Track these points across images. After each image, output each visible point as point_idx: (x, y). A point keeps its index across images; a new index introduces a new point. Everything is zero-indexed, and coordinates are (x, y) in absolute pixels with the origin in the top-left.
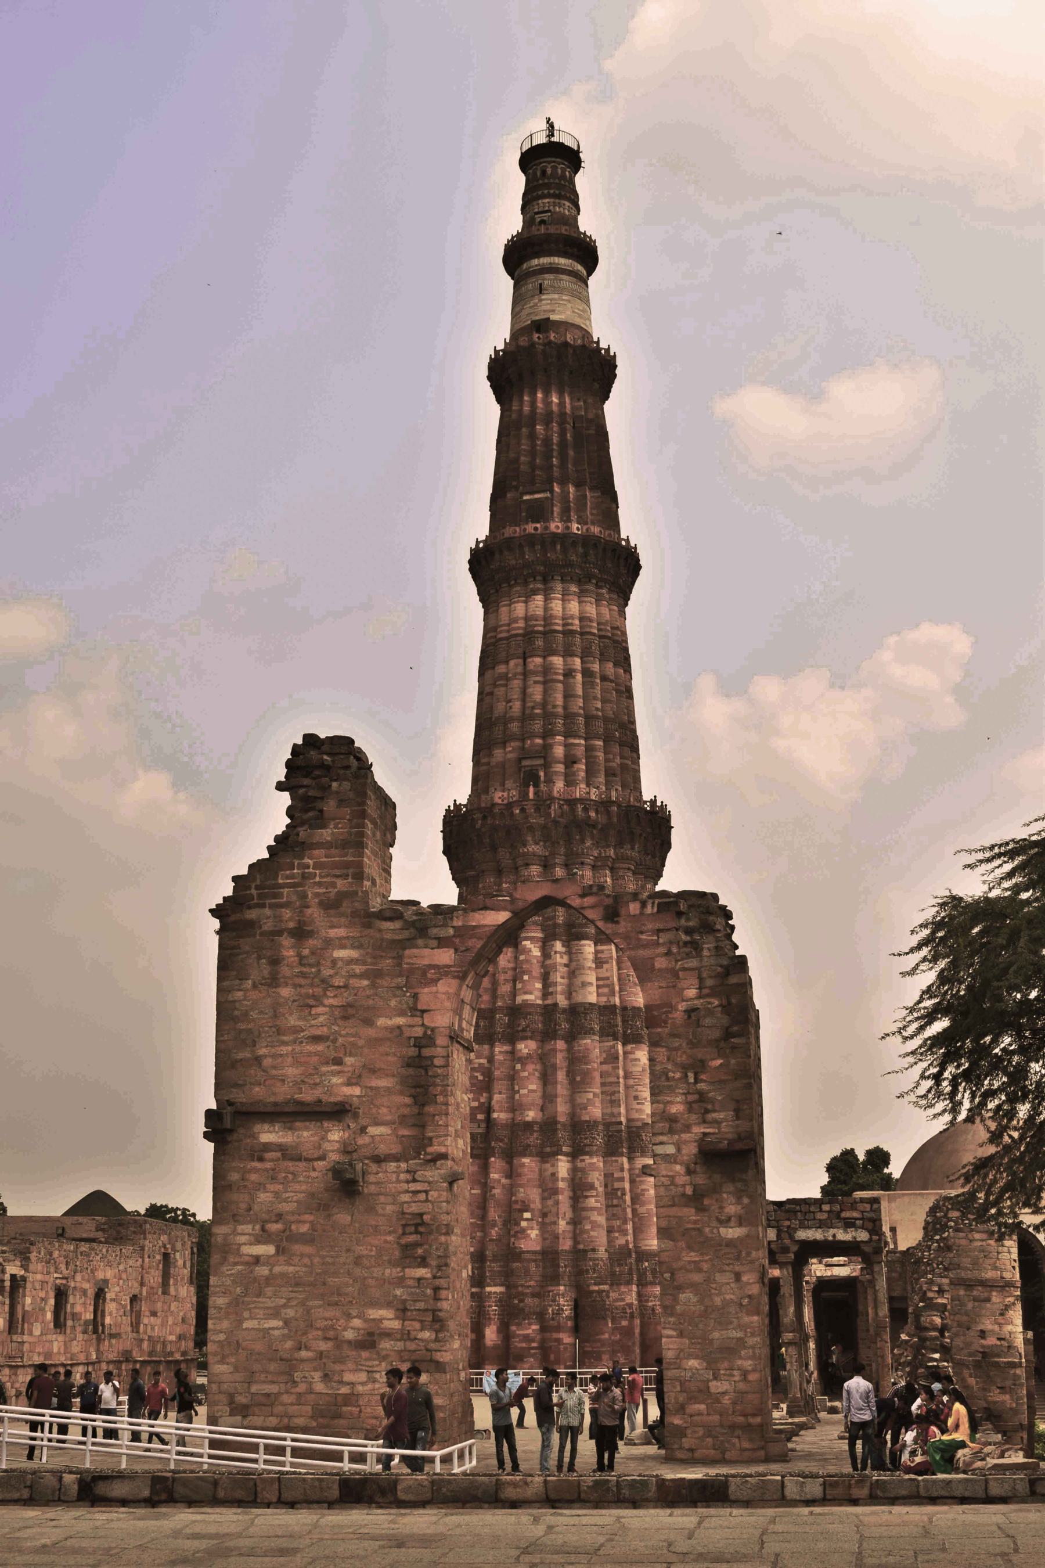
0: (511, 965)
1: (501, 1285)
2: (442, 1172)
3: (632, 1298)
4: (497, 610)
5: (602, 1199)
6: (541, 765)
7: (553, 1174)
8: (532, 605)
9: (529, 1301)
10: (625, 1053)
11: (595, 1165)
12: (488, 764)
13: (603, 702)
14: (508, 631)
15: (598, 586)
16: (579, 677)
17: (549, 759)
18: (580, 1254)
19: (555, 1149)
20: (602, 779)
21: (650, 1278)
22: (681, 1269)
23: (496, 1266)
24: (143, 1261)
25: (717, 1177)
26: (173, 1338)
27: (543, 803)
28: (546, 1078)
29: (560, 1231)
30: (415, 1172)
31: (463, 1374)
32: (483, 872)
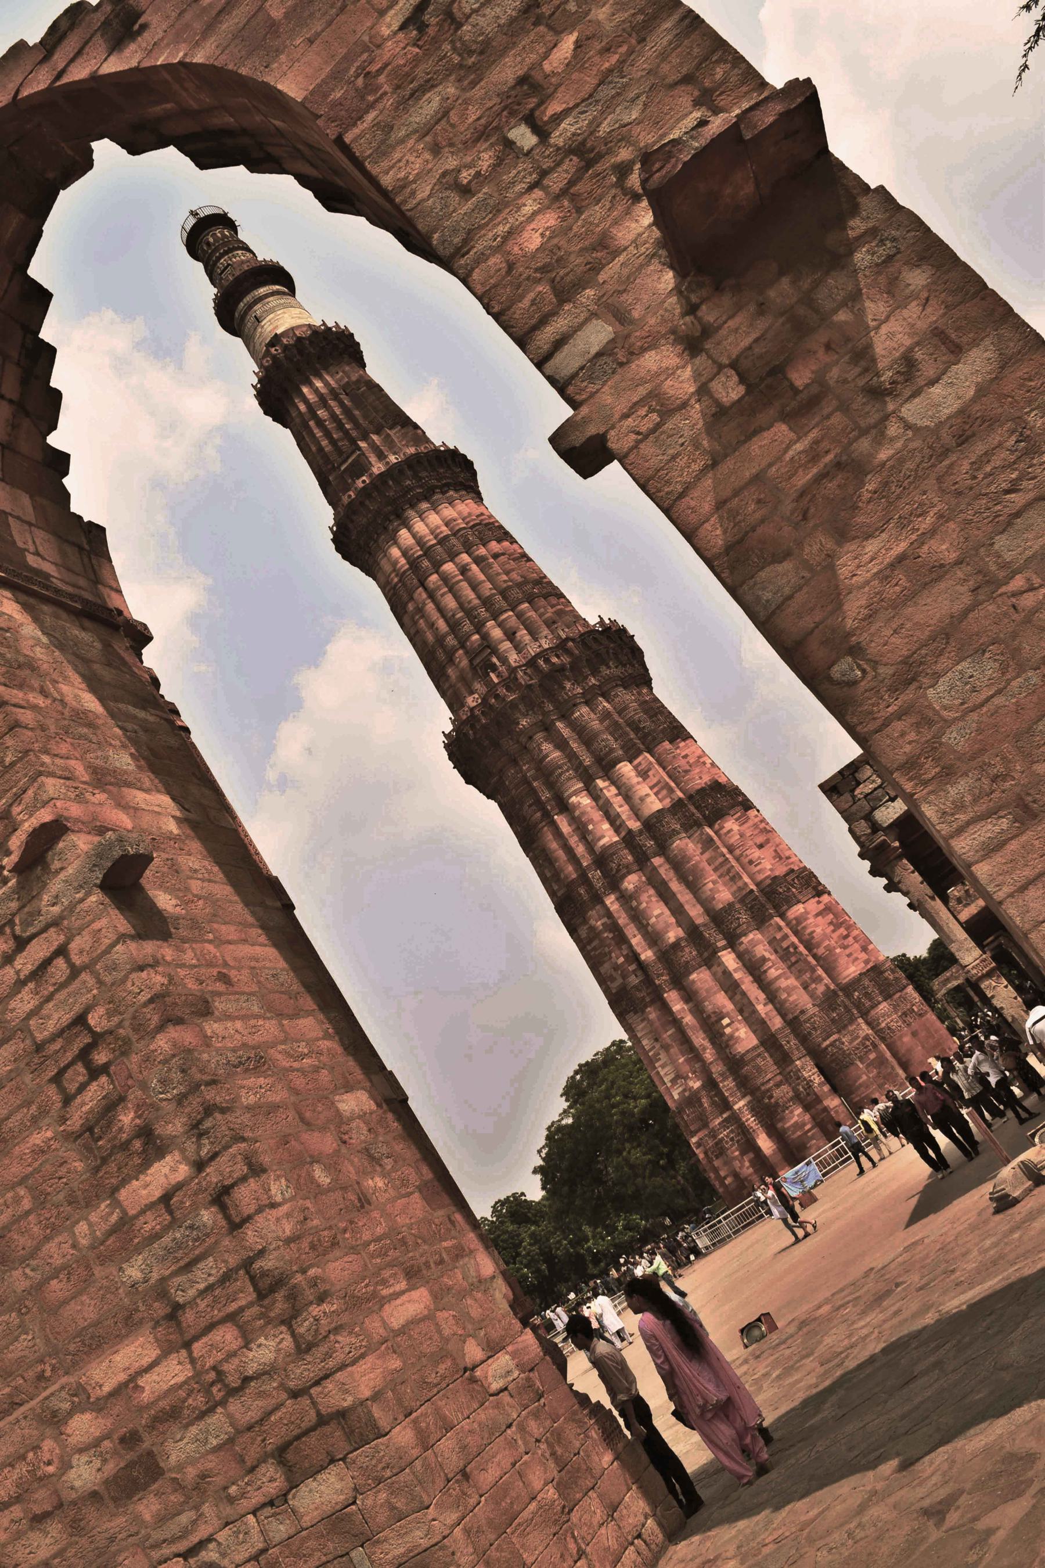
1: (743, 1097)
2: (70, 870)
3: (865, 1030)
8: (401, 541)
9: (777, 1093)
10: (716, 833)
11: (757, 942)
12: (451, 686)
13: (507, 573)
15: (444, 493)
16: (474, 567)
18: (793, 1023)
19: (710, 950)
20: (546, 631)
21: (868, 1004)
22: (870, 617)
25: (783, 291)
27: (510, 681)
28: (665, 895)
30: (11, 923)
31: (499, 1370)
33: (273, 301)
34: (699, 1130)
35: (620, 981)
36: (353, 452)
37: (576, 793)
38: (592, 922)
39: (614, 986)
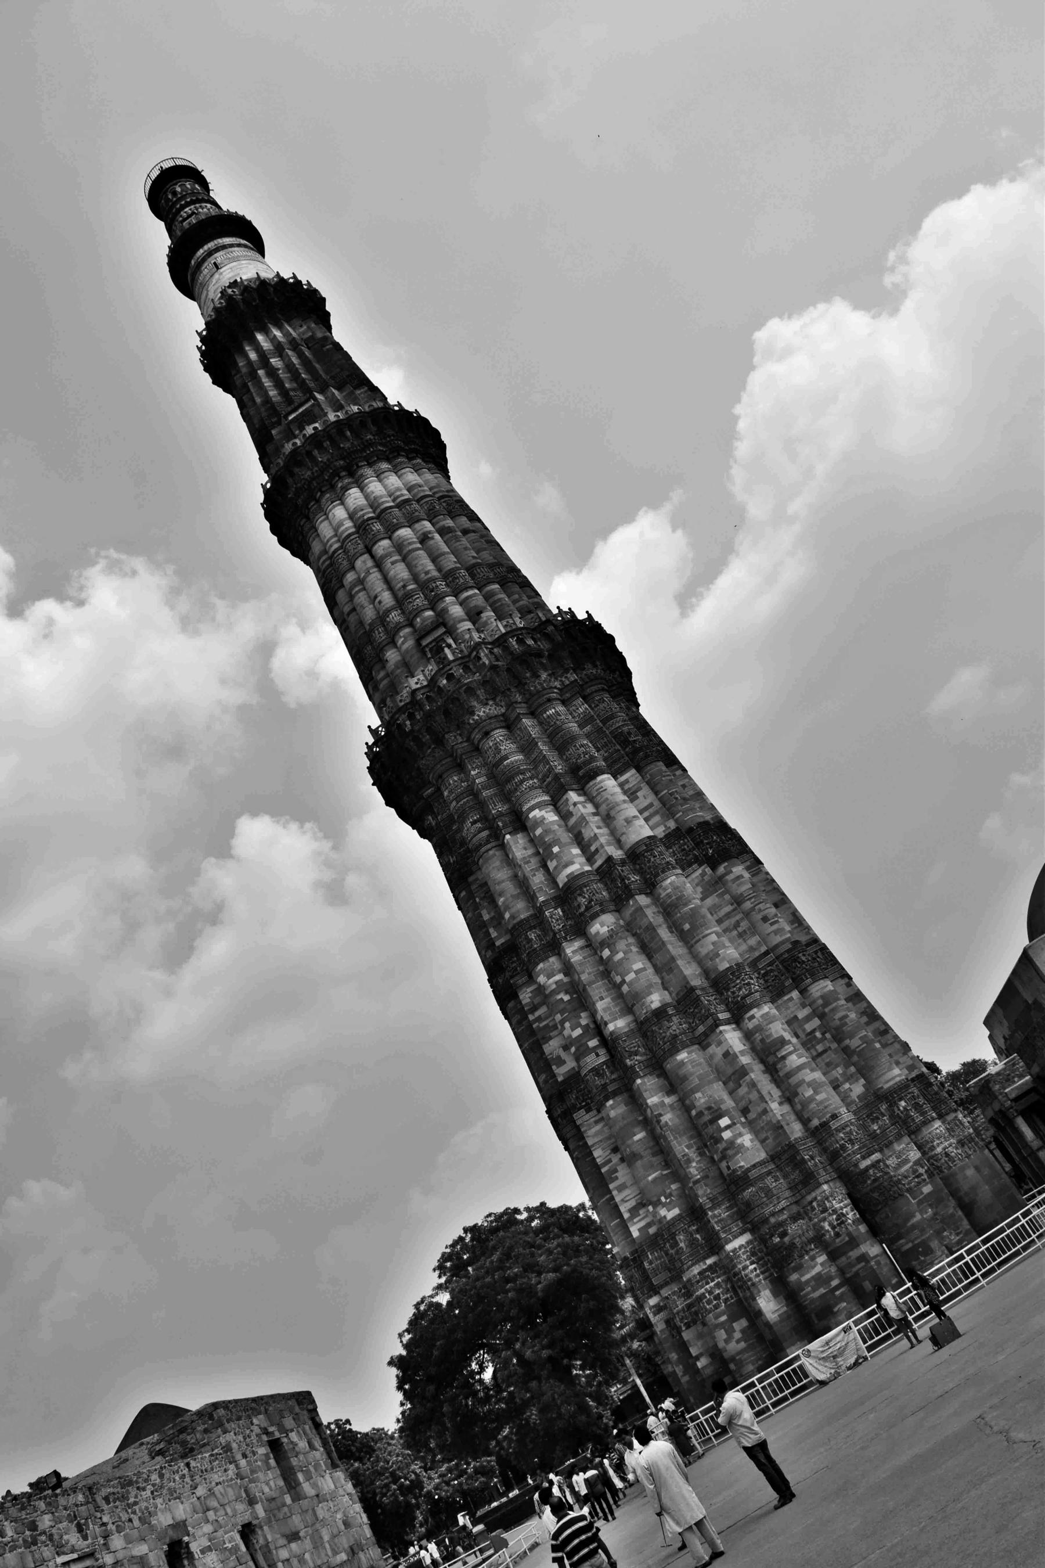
0: (530, 852)
1: (741, 1234)
4: (318, 535)
5: (802, 1051)
6: (444, 633)
7: (726, 1054)
9: (793, 1229)
14: (339, 541)
15: (410, 459)
16: (437, 536)
17: (451, 622)
21: (919, 1119)
24: (237, 1467)
26: (343, 1557)
28: (648, 948)
29: (780, 1118)
32: (440, 776)
33: (237, 251)
34: (666, 1284)
35: (570, 1064)
37: (539, 806)
38: (542, 979)
39: (560, 1073)
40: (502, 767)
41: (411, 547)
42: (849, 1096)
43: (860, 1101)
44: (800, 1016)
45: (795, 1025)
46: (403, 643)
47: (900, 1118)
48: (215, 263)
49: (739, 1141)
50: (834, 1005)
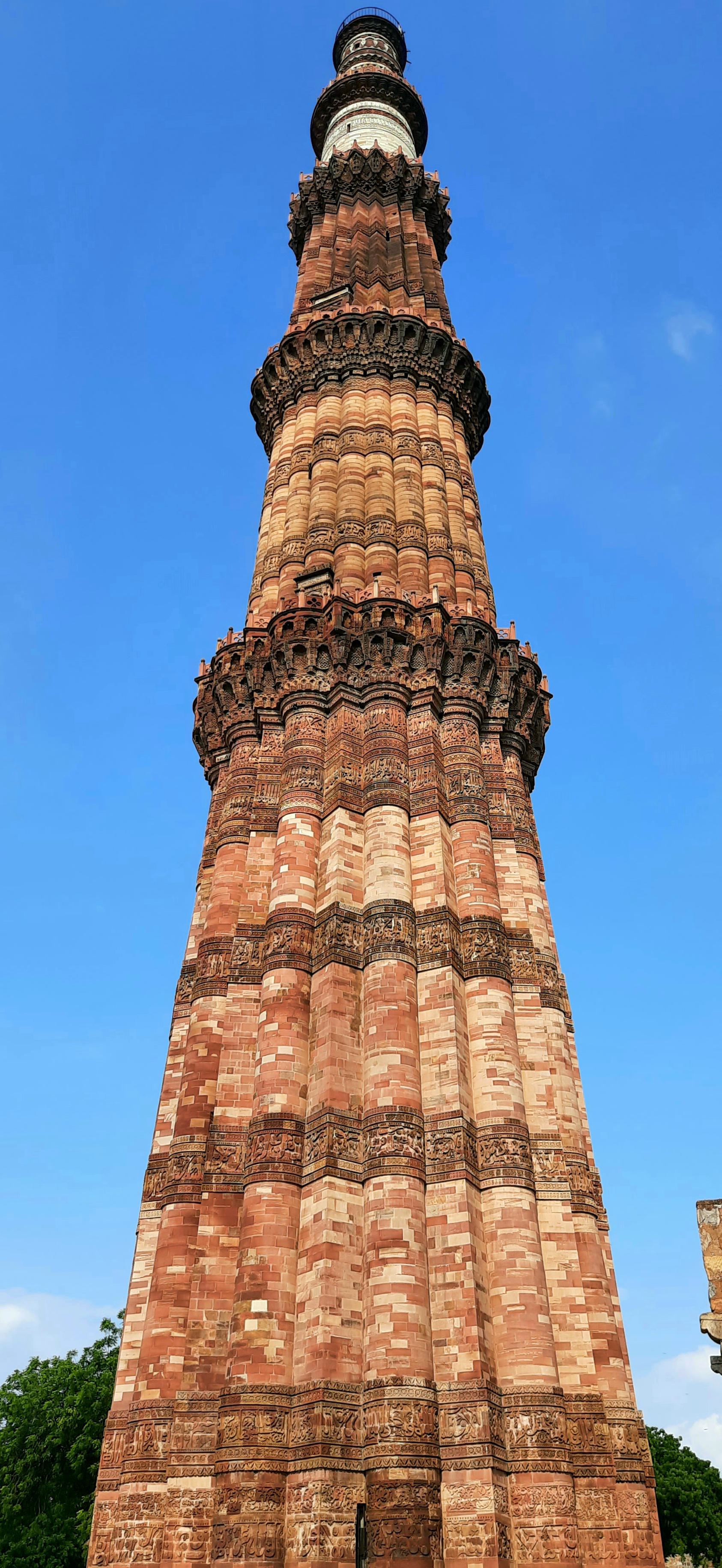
9: (249, 1507)
16: (387, 476)
23: (193, 1429)
33: (381, 119)
36: (343, 288)
37: (297, 811)
38: (194, 1017)
40: (289, 751)
41: (350, 477)
42: (449, 1366)
43: (458, 1382)
44: (450, 1220)
45: (439, 1227)
46: (283, 580)
47: (511, 1439)
48: (349, 126)
49: (259, 1342)
50: (517, 1230)
